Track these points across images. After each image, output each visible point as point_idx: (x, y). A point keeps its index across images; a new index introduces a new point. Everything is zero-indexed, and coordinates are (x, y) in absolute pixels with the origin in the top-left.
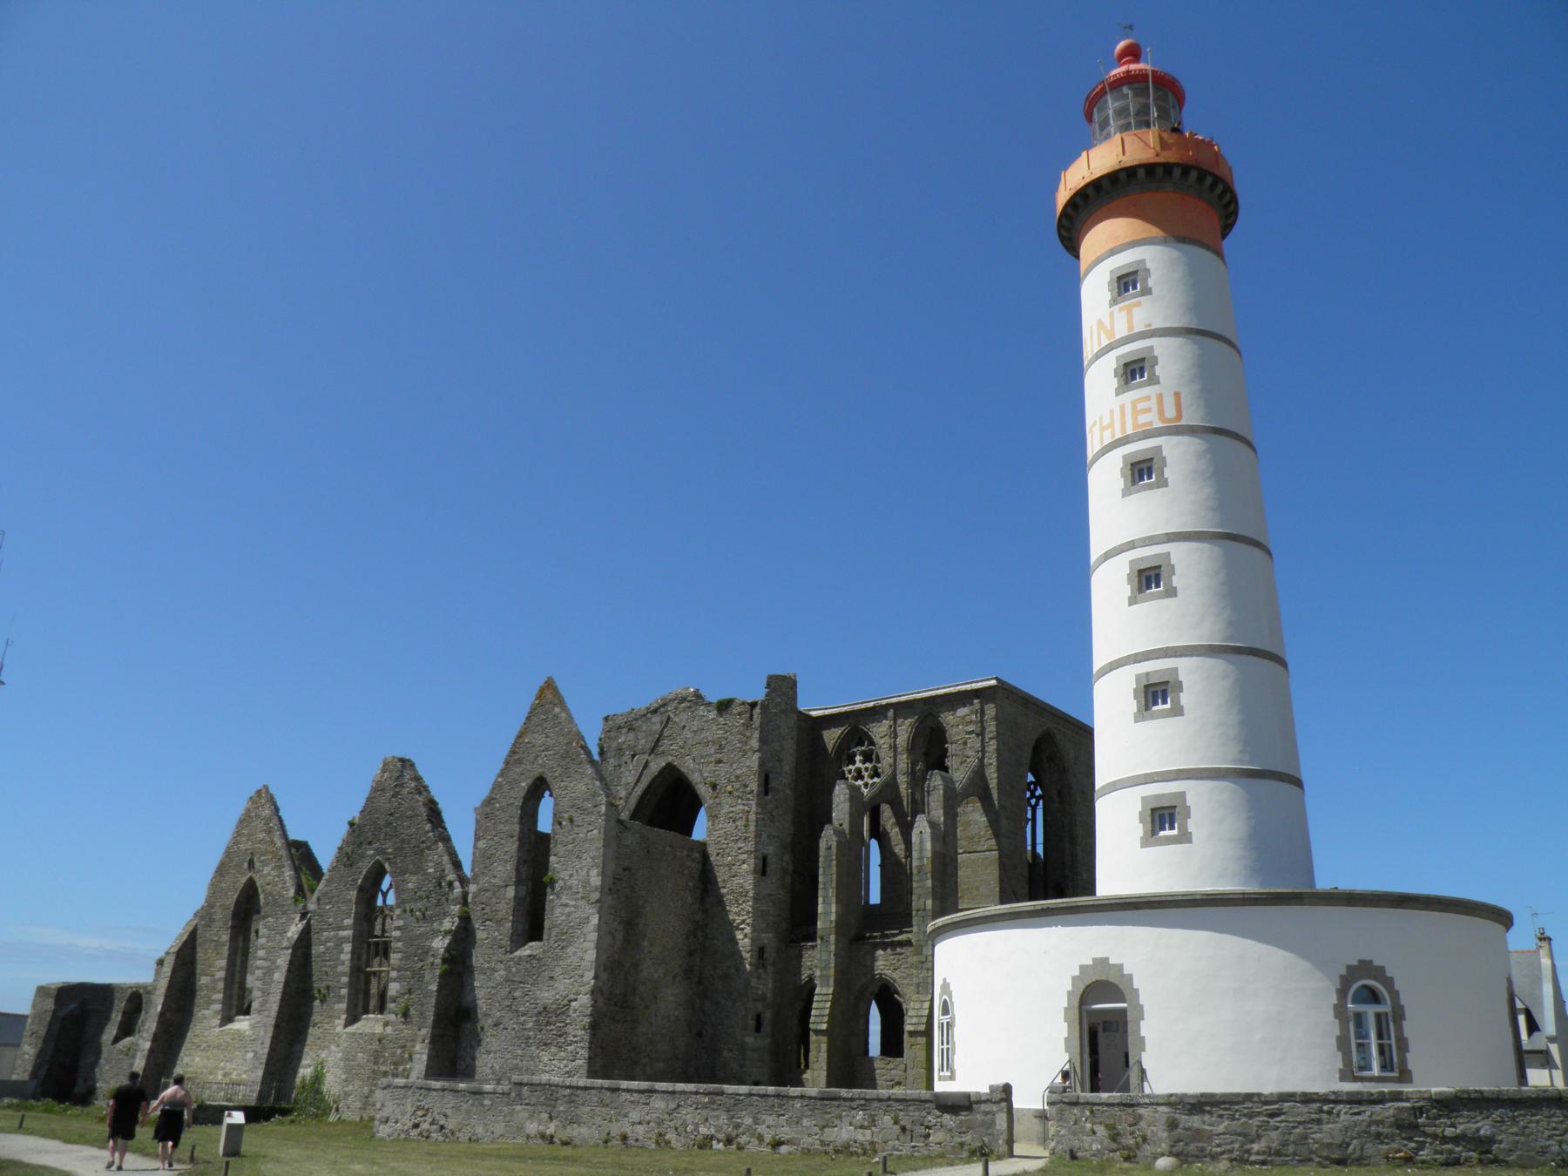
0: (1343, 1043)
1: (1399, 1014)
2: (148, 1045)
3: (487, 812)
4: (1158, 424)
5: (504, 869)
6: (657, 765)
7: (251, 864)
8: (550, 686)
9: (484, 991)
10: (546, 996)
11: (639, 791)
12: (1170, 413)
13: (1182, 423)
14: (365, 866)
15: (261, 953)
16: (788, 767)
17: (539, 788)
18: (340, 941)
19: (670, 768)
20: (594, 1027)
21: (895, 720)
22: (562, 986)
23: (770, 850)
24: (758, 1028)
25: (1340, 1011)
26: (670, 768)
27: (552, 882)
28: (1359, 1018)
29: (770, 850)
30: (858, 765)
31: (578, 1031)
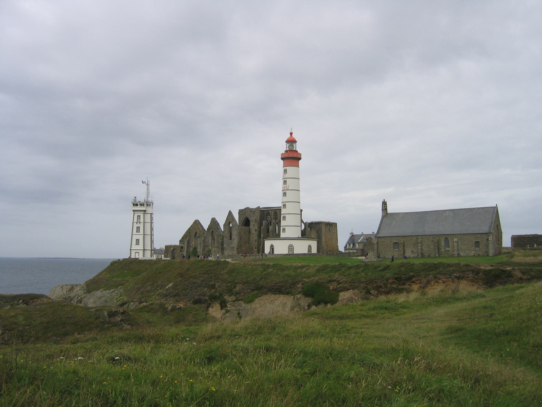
0: (288, 251)
1: (293, 248)
2: (186, 253)
3: (224, 225)
4: (286, 189)
5: (226, 232)
6: (245, 217)
7: (196, 230)
8: (230, 211)
9: (225, 246)
10: (232, 246)
11: (243, 220)
12: (287, 188)
13: (289, 189)
14: (211, 231)
15: (199, 241)
16: (259, 219)
17: (230, 223)
18: (209, 241)
19: (246, 217)
20: (238, 248)
21: (272, 211)
22: (234, 245)
23: (257, 228)
24: (256, 248)
25: (288, 248)
26: (246, 217)
27: (232, 234)
28: (290, 249)
29: (257, 228)
30: (269, 216)
31: (236, 250)
